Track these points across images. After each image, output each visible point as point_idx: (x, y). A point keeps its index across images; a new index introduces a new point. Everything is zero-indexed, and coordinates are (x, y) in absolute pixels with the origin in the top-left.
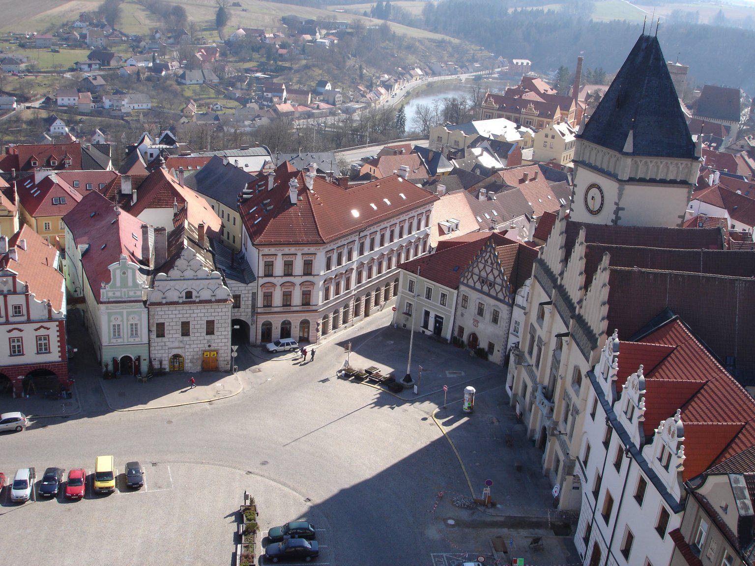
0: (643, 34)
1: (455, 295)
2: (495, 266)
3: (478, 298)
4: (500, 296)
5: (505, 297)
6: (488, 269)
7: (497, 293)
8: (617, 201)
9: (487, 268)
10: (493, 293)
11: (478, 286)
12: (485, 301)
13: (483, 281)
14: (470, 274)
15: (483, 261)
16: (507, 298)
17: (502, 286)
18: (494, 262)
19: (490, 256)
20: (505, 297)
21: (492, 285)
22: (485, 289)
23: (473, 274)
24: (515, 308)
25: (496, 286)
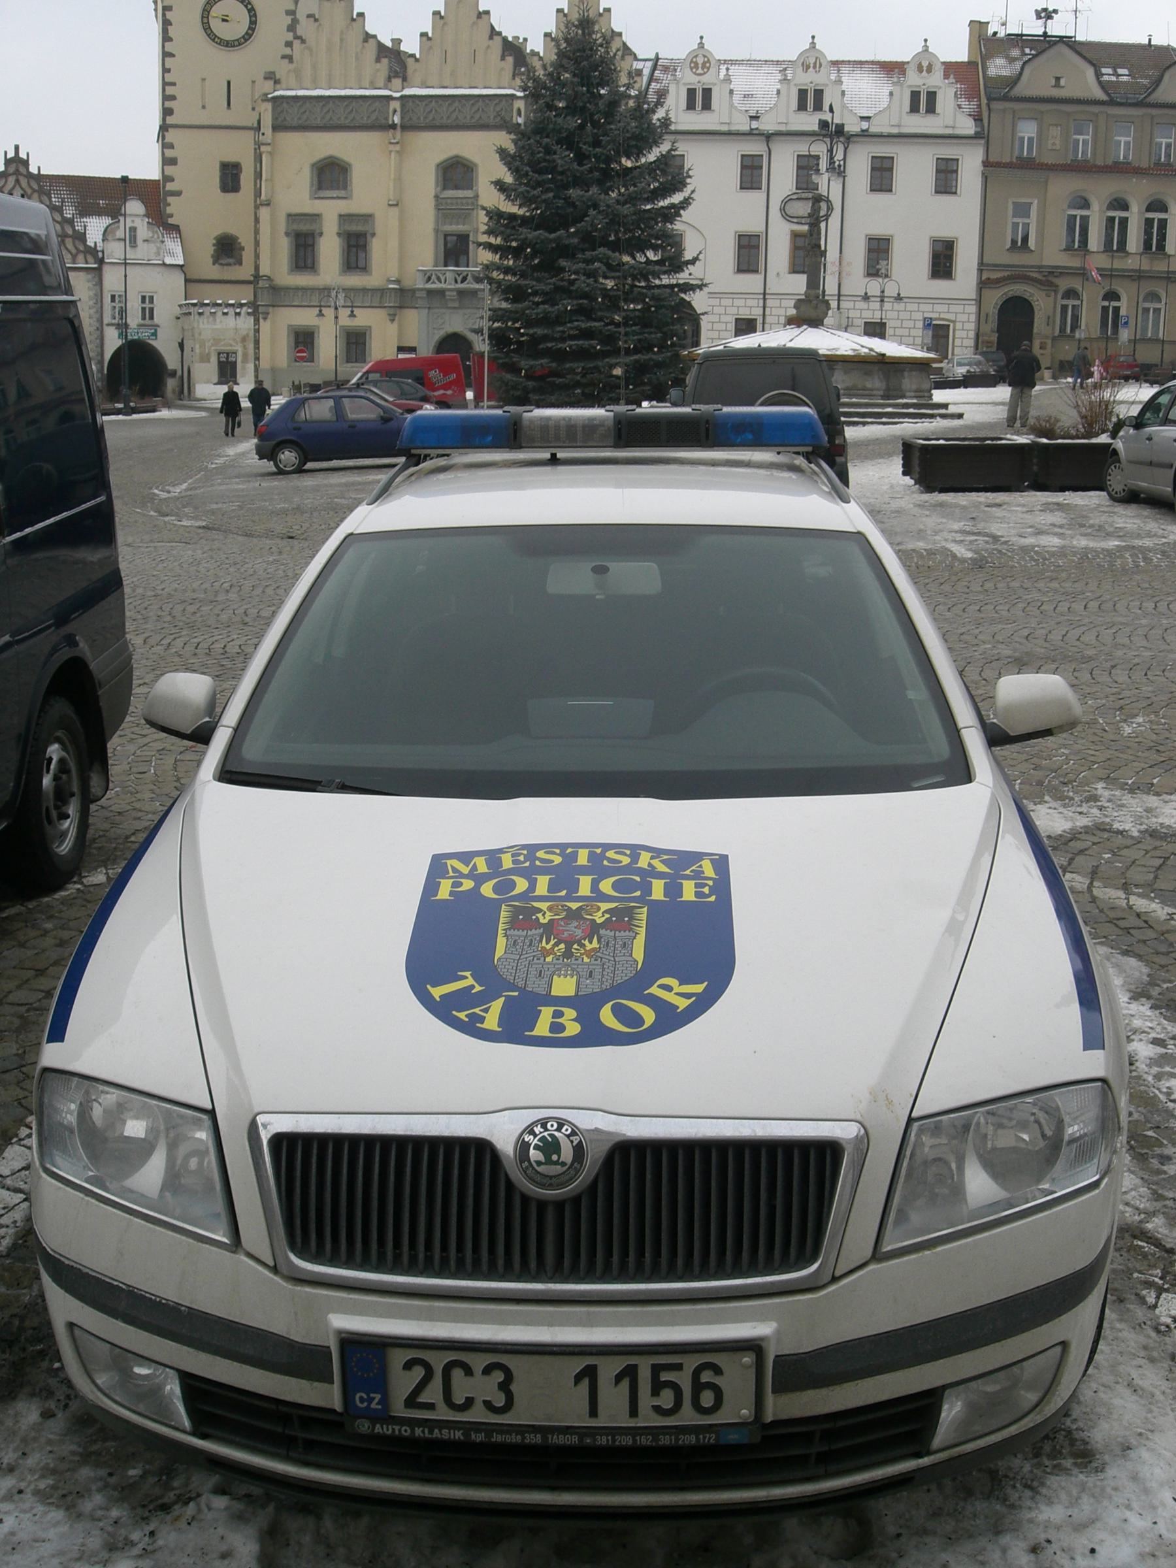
8: (292, 7)
18: (29, 191)
19: (17, 181)
24: (106, 268)
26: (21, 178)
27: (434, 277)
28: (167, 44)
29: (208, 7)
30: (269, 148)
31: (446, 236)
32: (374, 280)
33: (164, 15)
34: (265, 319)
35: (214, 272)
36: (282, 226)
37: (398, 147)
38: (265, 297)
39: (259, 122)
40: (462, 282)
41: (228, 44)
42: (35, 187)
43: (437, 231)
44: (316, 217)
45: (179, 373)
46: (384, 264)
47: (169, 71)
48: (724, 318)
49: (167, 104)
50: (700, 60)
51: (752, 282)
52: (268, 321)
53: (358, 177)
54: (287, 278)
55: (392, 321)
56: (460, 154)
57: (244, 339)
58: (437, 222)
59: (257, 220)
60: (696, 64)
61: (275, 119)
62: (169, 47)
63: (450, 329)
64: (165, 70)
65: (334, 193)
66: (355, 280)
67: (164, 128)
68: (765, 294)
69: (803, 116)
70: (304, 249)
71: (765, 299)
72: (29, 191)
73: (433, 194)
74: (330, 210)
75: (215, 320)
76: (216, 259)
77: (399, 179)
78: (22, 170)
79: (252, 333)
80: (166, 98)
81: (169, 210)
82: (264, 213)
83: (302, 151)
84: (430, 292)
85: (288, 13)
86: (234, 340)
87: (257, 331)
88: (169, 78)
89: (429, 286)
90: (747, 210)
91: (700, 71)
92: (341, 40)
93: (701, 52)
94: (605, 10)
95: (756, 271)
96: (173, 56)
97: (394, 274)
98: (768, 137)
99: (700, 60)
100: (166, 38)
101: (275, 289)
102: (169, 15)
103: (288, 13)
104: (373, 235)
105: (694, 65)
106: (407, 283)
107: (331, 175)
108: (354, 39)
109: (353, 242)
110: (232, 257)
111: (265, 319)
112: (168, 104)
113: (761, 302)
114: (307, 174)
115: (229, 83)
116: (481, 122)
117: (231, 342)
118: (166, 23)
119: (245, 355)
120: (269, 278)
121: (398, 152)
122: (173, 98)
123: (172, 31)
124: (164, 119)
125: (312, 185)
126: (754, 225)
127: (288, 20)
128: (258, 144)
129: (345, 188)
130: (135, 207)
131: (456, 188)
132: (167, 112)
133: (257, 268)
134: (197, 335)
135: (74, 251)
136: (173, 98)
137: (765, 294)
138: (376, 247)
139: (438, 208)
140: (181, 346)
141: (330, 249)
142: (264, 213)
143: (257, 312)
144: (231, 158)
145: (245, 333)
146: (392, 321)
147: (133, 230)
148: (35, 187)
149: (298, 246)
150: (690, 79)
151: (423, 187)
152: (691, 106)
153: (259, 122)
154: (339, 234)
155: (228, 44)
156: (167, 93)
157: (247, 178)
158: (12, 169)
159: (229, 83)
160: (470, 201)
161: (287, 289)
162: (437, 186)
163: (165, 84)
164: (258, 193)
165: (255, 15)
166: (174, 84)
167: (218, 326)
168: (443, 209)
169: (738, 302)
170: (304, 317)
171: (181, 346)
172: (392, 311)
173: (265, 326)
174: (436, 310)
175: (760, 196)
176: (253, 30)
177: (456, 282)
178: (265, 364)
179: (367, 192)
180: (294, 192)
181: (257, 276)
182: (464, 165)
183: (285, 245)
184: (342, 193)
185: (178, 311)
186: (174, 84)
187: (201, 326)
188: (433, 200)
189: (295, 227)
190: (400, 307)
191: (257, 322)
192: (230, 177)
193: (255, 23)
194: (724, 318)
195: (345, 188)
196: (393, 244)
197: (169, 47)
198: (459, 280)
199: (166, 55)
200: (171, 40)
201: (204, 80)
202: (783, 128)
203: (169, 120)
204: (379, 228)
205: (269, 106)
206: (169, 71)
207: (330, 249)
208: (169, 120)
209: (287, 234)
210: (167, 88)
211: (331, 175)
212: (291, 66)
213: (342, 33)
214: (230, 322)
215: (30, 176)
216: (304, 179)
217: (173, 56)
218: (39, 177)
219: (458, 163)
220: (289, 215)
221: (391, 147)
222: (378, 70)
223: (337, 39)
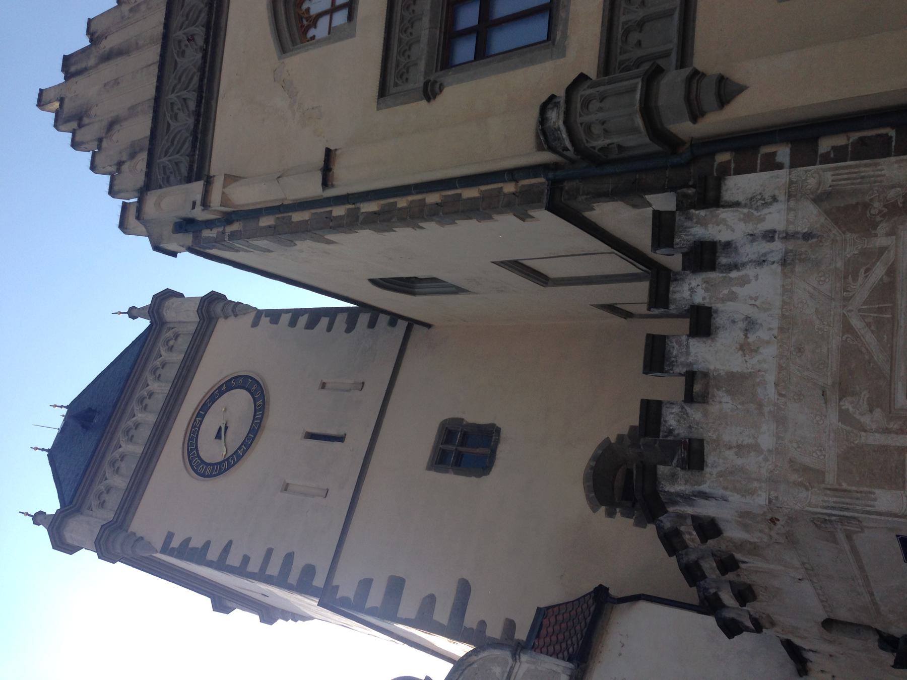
34: (726, 90)
47: (246, 559)
52: (737, 75)
75: (738, 383)
79: (817, 176)
86: (851, 272)
87: (803, 135)
102: (175, 544)
111: (726, 90)
117: (862, 289)
123: (197, 543)
144: (425, 442)
145: (809, 216)
191: (749, 146)
210: (268, 572)
214: (752, 293)
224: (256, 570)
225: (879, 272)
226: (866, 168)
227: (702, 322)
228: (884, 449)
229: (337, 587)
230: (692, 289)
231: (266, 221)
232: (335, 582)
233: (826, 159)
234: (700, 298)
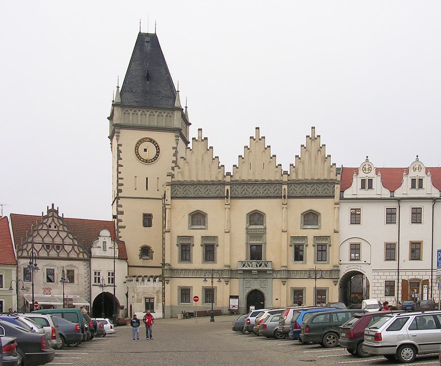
0: (140, 32)
1: (14, 272)
2: (61, 228)
3: (45, 266)
4: (73, 255)
5: (78, 255)
6: (53, 234)
7: (68, 254)
9: (50, 233)
10: (63, 255)
11: (43, 254)
12: (55, 266)
13: (48, 246)
14: (30, 246)
15: (45, 227)
16: (81, 254)
17: (73, 245)
18: (58, 225)
20: (78, 255)
21: (58, 247)
22: (53, 253)
23: (33, 243)
24: (92, 260)
25: (66, 247)
26: (54, 218)
27: (246, 264)
28: (119, 161)
29: (138, 145)
30: (169, 207)
31: (251, 246)
32: (218, 265)
33: (118, 148)
34: (167, 283)
35: (140, 262)
36: (175, 242)
37: (229, 206)
38: (166, 274)
39: (165, 195)
40: (259, 267)
41: (147, 161)
42: (61, 223)
43: (247, 244)
44: (191, 237)
45: (125, 307)
46: (223, 258)
47: (120, 173)
48: (380, 281)
49: (119, 188)
50: (367, 167)
51: (392, 265)
53: (210, 219)
54: (177, 265)
55: (227, 284)
56: (258, 209)
57: (157, 292)
58: (247, 240)
59: (164, 239)
60: (365, 168)
61: (172, 193)
62: (120, 162)
63: (254, 288)
64: (119, 173)
65: (199, 227)
66: (209, 266)
67: (117, 198)
68: (398, 270)
69: (414, 191)
70: (185, 251)
71: (398, 272)
72: (58, 225)
73: (245, 227)
74: (197, 235)
76: (141, 257)
77: (229, 221)
78: (56, 216)
79: (161, 290)
80: (119, 185)
81: (120, 235)
82: (167, 235)
83: (184, 208)
84: (244, 271)
85: (174, 148)
88: (120, 176)
89: (244, 268)
90: (389, 234)
91: (367, 172)
92: (202, 159)
93: (367, 163)
94: (323, 145)
95: (394, 260)
96: (123, 166)
97: (228, 263)
98: (399, 200)
99: (367, 167)
100: (119, 158)
101: (172, 270)
103: (174, 148)
104: (218, 245)
105: (364, 169)
106: (234, 267)
107: (198, 218)
108: (207, 159)
109: (184, 249)
110: (148, 256)
111: (167, 283)
112: (119, 188)
113: (397, 273)
114: (186, 219)
115: (147, 178)
116: (267, 195)
118: (119, 152)
119: (158, 300)
120: (169, 265)
121: (229, 208)
122: (122, 185)
124: (118, 194)
125: (189, 223)
126: (394, 240)
127: (174, 151)
128: (165, 205)
129: (204, 225)
130: (105, 233)
131: (256, 224)
132: (119, 191)
133: (164, 260)
134: (135, 290)
135: (78, 252)
136: (122, 185)
137: (398, 270)
138: (219, 252)
139: (247, 234)
140: (127, 295)
141: (197, 252)
142: (167, 235)
143: (163, 279)
146: (227, 284)
147: (105, 243)
148: (61, 223)
149: (182, 251)
150: (362, 175)
151: (240, 225)
152: (363, 187)
153: (165, 195)
154: (202, 245)
155: (147, 161)
156: (120, 182)
157: (156, 221)
158: (50, 215)
159: (147, 178)
160: (262, 230)
161: (177, 270)
162: (247, 223)
163: (118, 179)
164: (164, 227)
165: (159, 149)
166: (122, 179)
167: (145, 286)
168: (250, 234)
169: (386, 274)
170: (185, 283)
171: (127, 295)
172: (227, 280)
173: (167, 286)
174: (247, 279)
175: (395, 226)
176: (158, 155)
177: (257, 266)
178: (167, 304)
179: (214, 227)
180: (180, 225)
181: (164, 264)
182: (259, 214)
183: (176, 250)
184: (203, 227)
185: (125, 280)
186: (122, 179)
187: (137, 286)
188: (245, 229)
189: (181, 242)
190: (230, 278)
192: (147, 220)
193: (159, 152)
194: (380, 281)
195: (204, 225)
196: (227, 250)
197: (120, 162)
198: (258, 265)
199: (119, 166)
200: (121, 159)
201: (136, 177)
202: (405, 196)
203: (120, 195)
204: (220, 242)
205: (169, 187)
206: (120, 173)
207: (197, 252)
208: (120, 195)
209: (177, 245)
210: (119, 180)
211: (198, 218)
212: (179, 170)
213: (203, 155)
214: (151, 284)
215: (59, 218)
216: (186, 220)
217: (123, 166)
218: (62, 219)
219: (256, 213)
220: (178, 237)
221: (226, 206)
222: (219, 172)
223: (200, 159)
224: (119, 177)
225: (153, 294)
226: (161, 293)
227: (149, 281)
228: (139, 295)
229: (119, 199)
230: (151, 279)
231: (164, 214)
232: (120, 199)
233: (162, 290)
234: (151, 280)
